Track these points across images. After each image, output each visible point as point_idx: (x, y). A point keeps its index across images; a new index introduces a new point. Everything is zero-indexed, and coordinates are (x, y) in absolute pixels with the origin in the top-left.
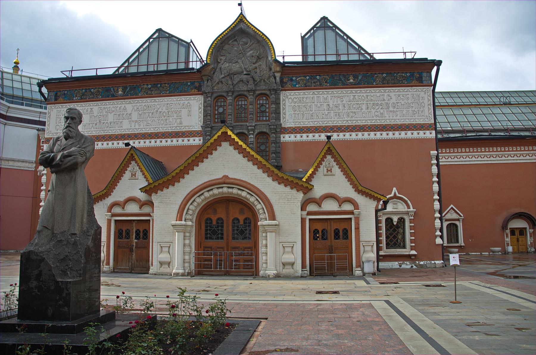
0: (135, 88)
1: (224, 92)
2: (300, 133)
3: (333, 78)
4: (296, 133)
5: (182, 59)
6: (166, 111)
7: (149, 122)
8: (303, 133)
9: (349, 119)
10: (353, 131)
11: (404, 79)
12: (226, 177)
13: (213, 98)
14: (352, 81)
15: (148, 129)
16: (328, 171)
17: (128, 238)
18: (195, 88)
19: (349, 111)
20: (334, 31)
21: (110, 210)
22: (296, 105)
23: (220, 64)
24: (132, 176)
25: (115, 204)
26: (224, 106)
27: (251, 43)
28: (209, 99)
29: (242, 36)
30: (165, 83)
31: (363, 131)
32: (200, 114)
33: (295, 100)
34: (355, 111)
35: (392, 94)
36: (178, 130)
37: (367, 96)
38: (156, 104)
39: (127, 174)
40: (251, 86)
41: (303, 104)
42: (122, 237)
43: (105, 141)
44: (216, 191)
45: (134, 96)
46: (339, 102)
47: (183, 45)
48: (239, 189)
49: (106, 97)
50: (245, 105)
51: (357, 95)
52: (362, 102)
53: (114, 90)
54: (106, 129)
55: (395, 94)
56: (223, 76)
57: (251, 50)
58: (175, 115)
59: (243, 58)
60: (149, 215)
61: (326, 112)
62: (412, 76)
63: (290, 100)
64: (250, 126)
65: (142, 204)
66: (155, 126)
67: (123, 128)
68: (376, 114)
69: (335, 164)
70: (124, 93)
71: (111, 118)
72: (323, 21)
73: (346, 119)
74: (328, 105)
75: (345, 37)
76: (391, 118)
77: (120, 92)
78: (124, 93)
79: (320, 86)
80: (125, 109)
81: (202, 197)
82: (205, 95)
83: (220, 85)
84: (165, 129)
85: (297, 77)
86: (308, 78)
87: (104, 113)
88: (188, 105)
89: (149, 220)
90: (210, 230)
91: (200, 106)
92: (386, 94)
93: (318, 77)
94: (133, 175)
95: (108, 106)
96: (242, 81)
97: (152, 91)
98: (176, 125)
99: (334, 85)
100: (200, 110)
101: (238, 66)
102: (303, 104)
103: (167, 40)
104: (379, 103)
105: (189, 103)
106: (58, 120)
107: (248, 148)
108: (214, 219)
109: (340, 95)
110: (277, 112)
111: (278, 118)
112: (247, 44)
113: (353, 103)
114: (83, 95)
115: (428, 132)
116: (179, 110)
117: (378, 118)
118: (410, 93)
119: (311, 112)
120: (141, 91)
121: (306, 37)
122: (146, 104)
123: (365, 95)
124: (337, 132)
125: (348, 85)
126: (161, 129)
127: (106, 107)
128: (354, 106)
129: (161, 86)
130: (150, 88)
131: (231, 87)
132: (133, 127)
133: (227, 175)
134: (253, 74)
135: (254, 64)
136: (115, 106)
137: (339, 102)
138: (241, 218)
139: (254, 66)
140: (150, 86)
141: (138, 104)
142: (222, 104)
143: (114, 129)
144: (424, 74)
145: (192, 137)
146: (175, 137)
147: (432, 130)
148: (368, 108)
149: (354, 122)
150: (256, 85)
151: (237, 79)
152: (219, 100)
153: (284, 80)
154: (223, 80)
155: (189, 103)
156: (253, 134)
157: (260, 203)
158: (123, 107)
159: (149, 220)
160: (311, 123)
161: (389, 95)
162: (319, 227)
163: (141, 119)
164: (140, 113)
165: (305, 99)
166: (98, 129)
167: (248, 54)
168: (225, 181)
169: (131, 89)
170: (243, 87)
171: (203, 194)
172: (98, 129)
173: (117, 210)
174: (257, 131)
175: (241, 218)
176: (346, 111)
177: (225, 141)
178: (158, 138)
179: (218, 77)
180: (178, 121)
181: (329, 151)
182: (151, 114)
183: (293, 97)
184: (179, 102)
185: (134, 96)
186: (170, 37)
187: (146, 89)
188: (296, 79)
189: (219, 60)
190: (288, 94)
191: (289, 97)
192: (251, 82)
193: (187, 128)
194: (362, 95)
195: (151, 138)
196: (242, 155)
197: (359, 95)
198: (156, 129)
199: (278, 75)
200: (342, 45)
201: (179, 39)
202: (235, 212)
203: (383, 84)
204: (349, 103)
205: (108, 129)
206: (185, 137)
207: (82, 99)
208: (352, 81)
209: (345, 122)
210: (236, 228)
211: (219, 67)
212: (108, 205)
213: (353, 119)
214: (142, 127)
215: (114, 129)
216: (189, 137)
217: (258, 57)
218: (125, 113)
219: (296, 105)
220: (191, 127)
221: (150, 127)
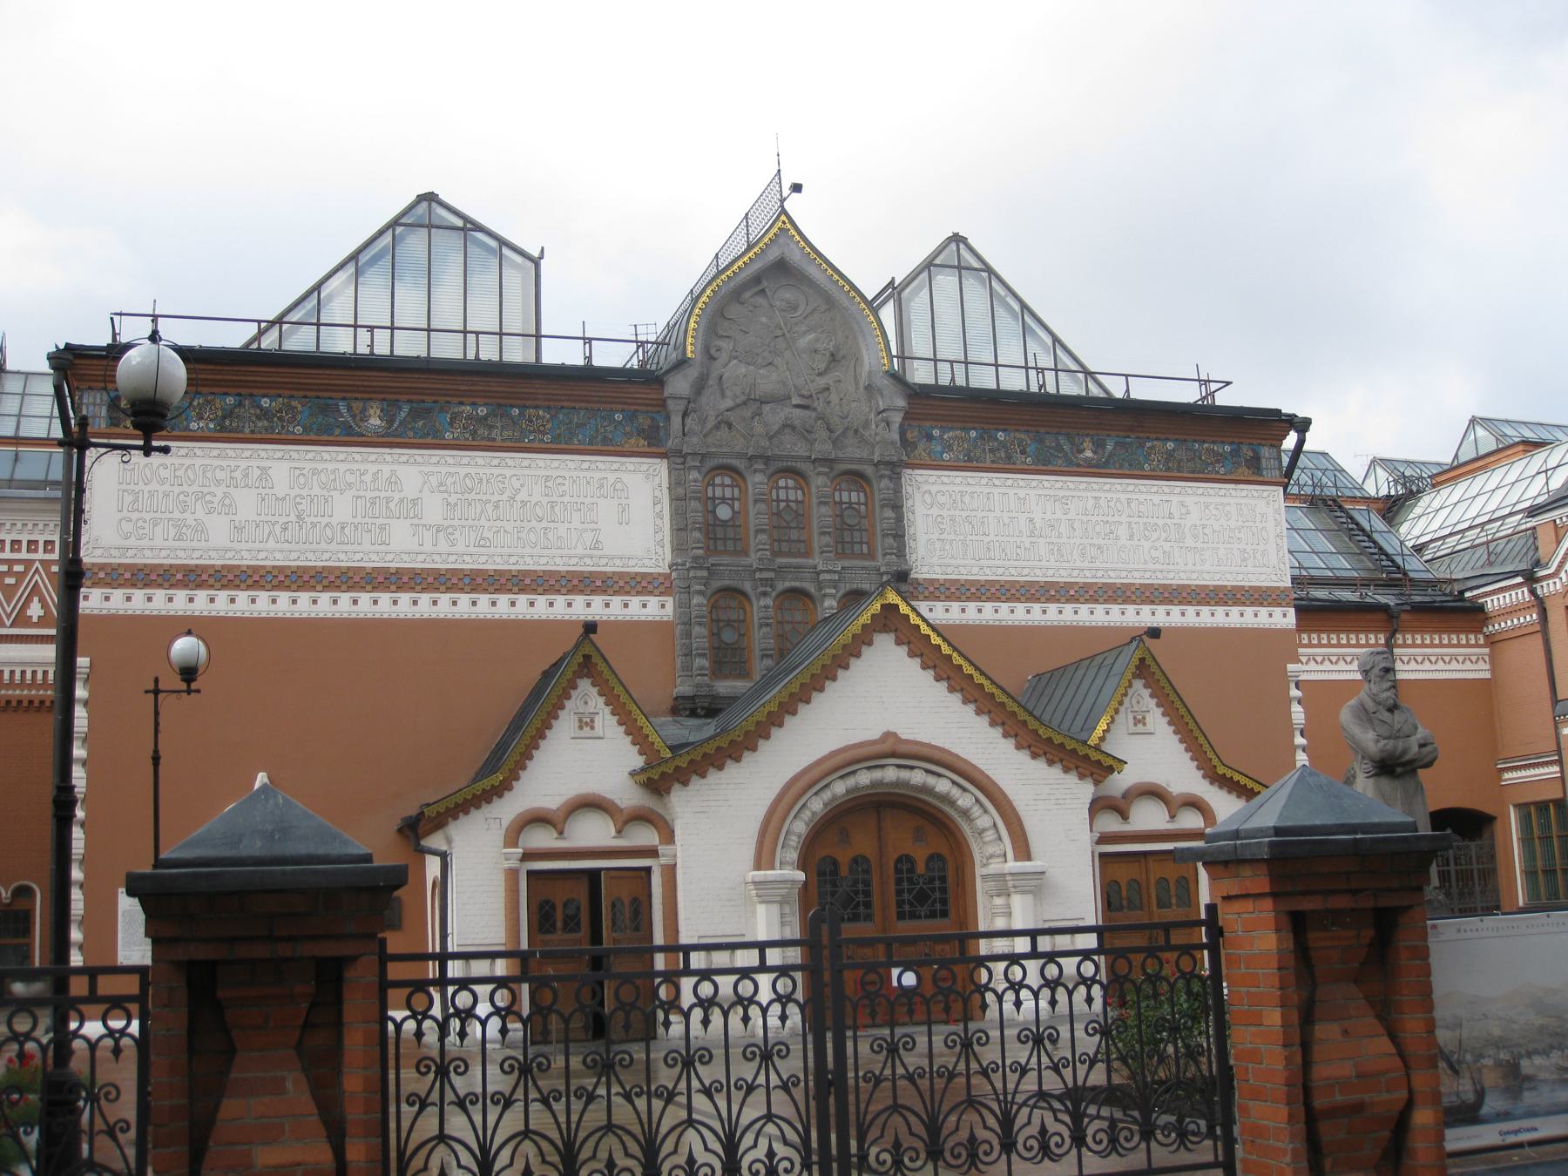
0: (429, 411)
1: (740, 456)
2: (958, 599)
3: (1041, 441)
4: (948, 598)
7: (490, 535)
8: (968, 599)
9: (1086, 564)
10: (1096, 601)
11: (1218, 461)
12: (888, 735)
13: (704, 470)
14: (1089, 454)
15: (483, 559)
16: (1137, 722)
17: (572, 931)
18: (641, 432)
19: (1085, 541)
20: (982, 281)
21: (513, 836)
22: (945, 513)
23: (717, 364)
24: (581, 728)
25: (538, 819)
26: (733, 499)
27: (810, 309)
28: (694, 475)
29: (773, 278)
30: (537, 407)
31: (1124, 602)
32: (659, 522)
33: (941, 499)
34: (1100, 541)
35: (1190, 500)
36: (587, 566)
37: (1129, 501)
38: (508, 472)
39: (565, 725)
40: (823, 447)
41: (964, 514)
42: (554, 925)
43: (326, 588)
44: (864, 778)
45: (429, 440)
46: (1059, 515)
47: (515, 265)
48: (927, 771)
49: (320, 431)
50: (796, 501)
51: (1102, 495)
52: (1116, 518)
53: (349, 409)
54: (323, 546)
55: (1197, 499)
56: (729, 403)
57: (810, 330)
58: (576, 517)
59: (787, 354)
60: (652, 853)
61: (1027, 541)
62: (1235, 453)
64: (828, 572)
65: (629, 819)
66: (506, 551)
67: (392, 547)
68: (1155, 554)
69: (1152, 703)
70: (390, 422)
71: (342, 508)
72: (953, 246)
73: (1078, 564)
74: (1031, 520)
75: (1017, 307)
76: (1190, 567)
77: (375, 422)
78: (390, 422)
79: (1006, 464)
80: (394, 481)
81: (827, 795)
82: (680, 460)
83: (724, 433)
84: (543, 560)
85: (943, 430)
86: (973, 434)
87: (316, 490)
89: (648, 870)
90: (910, 891)
91: (657, 493)
92: (1175, 499)
93: (1001, 435)
94: (586, 723)
95: (331, 466)
96: (793, 428)
97: (491, 428)
98: (580, 551)
99: (1044, 465)
100: (658, 508)
101: (774, 376)
102: (964, 514)
103: (456, 240)
104: (1161, 522)
105: (619, 480)
106: (128, 498)
107: (955, 655)
108: (844, 857)
109: (1062, 493)
110: (898, 534)
111: (901, 552)
112: (795, 308)
113: (1094, 519)
114: (229, 414)
115: (1278, 611)
116: (588, 500)
117: (1158, 566)
118: (1232, 501)
119: (986, 539)
120: (451, 424)
122: (473, 471)
123: (1123, 497)
124: (1058, 601)
125: (1079, 465)
126: (528, 560)
127: (320, 466)
128: (1098, 529)
130: (485, 418)
131: (765, 443)
132: (428, 547)
133: (892, 729)
134: (819, 405)
135: (820, 374)
136: (355, 467)
137: (1059, 515)
138: (920, 855)
139: (822, 382)
140: (482, 411)
141: (444, 470)
142: (728, 494)
143: (356, 547)
144: (1265, 452)
145: (638, 593)
146: (581, 592)
147: (1288, 605)
148: (1131, 537)
149: (1100, 574)
150: (834, 442)
151: (775, 416)
152: (718, 480)
153: (909, 436)
154: (732, 416)
155: (619, 480)
156: (833, 596)
157: (986, 811)
158: (387, 473)
159: (648, 870)
160: (987, 571)
161: (1182, 504)
162: (1123, 874)
163: (456, 523)
164: (453, 499)
165: (967, 499)
166: (293, 546)
167: (803, 342)
168: (893, 750)
169: (415, 415)
170: (795, 447)
171: (826, 786)
172: (293, 546)
173: (541, 839)
174: (845, 588)
175: (920, 855)
176: (1078, 541)
177: (885, 629)
178: (522, 591)
179: (714, 404)
180: (588, 537)
181: (1144, 669)
182: (490, 507)
183: (934, 489)
184: (588, 474)
185: (429, 440)
186: (470, 227)
187: (469, 417)
188: (941, 436)
189: (713, 351)
190: (919, 479)
191: (925, 487)
192: (824, 434)
193: (618, 562)
194: (1115, 496)
195: (497, 591)
196: (932, 672)
197: (1109, 495)
198: (513, 560)
199: (897, 418)
200: (1008, 327)
201: (503, 242)
202: (902, 840)
203: (1168, 469)
204: (1085, 518)
205: (333, 547)
206: (616, 593)
207: (223, 429)
208: (1089, 454)
209: (1075, 573)
210: (906, 885)
211: (714, 375)
212: (506, 822)
213: (1097, 564)
214: (460, 548)
215: (356, 547)
216: (628, 593)
217: (832, 355)
218: (397, 496)
219: (945, 513)
220: (632, 563)
221: (492, 550)
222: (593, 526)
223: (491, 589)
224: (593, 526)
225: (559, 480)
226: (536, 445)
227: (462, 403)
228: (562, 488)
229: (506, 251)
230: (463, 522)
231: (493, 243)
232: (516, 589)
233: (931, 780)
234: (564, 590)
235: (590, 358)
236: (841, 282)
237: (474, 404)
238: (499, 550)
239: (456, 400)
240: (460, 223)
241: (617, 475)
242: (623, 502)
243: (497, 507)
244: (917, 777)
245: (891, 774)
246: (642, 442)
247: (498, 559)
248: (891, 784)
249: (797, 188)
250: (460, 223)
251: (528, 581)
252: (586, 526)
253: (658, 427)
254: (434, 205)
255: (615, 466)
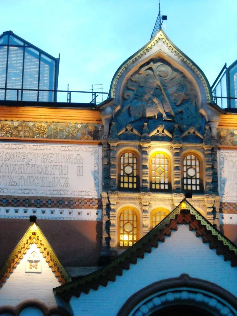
5: (45, 84)
6: (43, 164)
12: (184, 276)
15: (13, 191)
32: (97, 174)
38: (26, 152)
44: (171, 297)
63: (231, 164)
66: (23, 187)
81: (150, 305)
84: (41, 192)
88: (78, 158)
103: (20, 51)
107: (219, 236)
121: (233, 69)
129: (34, 125)
133: (186, 272)
140: (16, 124)
145: (85, 208)
168: (184, 282)
171: (151, 300)
177: (184, 222)
178: (30, 206)
182: (17, 167)
186: (26, 46)
187: (9, 127)
191: (229, 159)
195: (18, 206)
198: (27, 191)
201: (41, 52)
221: (17, 187)
222: (65, 176)
223: (15, 205)
224: (65, 176)
225: (50, 155)
226: (40, 139)
227: (6, 120)
228: (51, 159)
229: (43, 56)
230: (4, 174)
231: (38, 53)
232: (27, 205)
233: (206, 300)
234: (50, 206)
235: (70, 100)
236: (188, 62)
237: (12, 121)
238: (20, 187)
239: (3, 119)
240: (22, 44)
241: (79, 153)
242: (80, 165)
243: (20, 167)
244: (199, 298)
245: (185, 295)
246: (90, 137)
247: (20, 191)
248: (185, 301)
249: (165, 18)
250: (22, 44)
251: (33, 201)
252: (62, 176)
253: (98, 131)
254: (11, 37)
255: (77, 149)
